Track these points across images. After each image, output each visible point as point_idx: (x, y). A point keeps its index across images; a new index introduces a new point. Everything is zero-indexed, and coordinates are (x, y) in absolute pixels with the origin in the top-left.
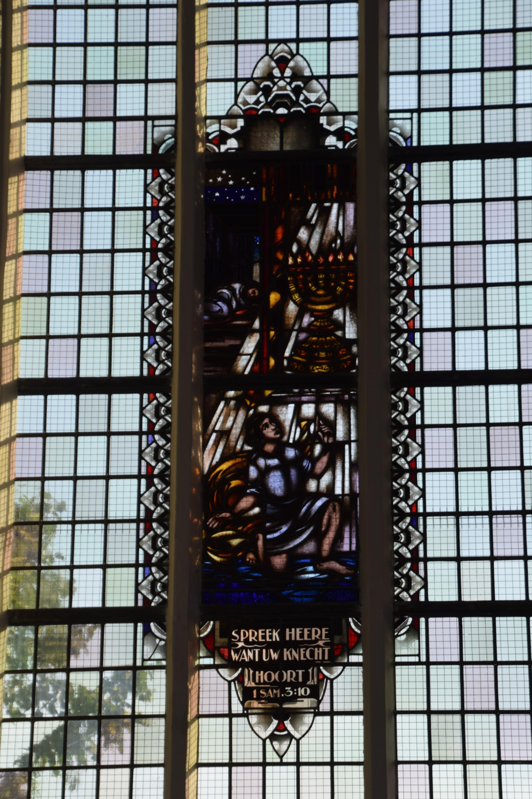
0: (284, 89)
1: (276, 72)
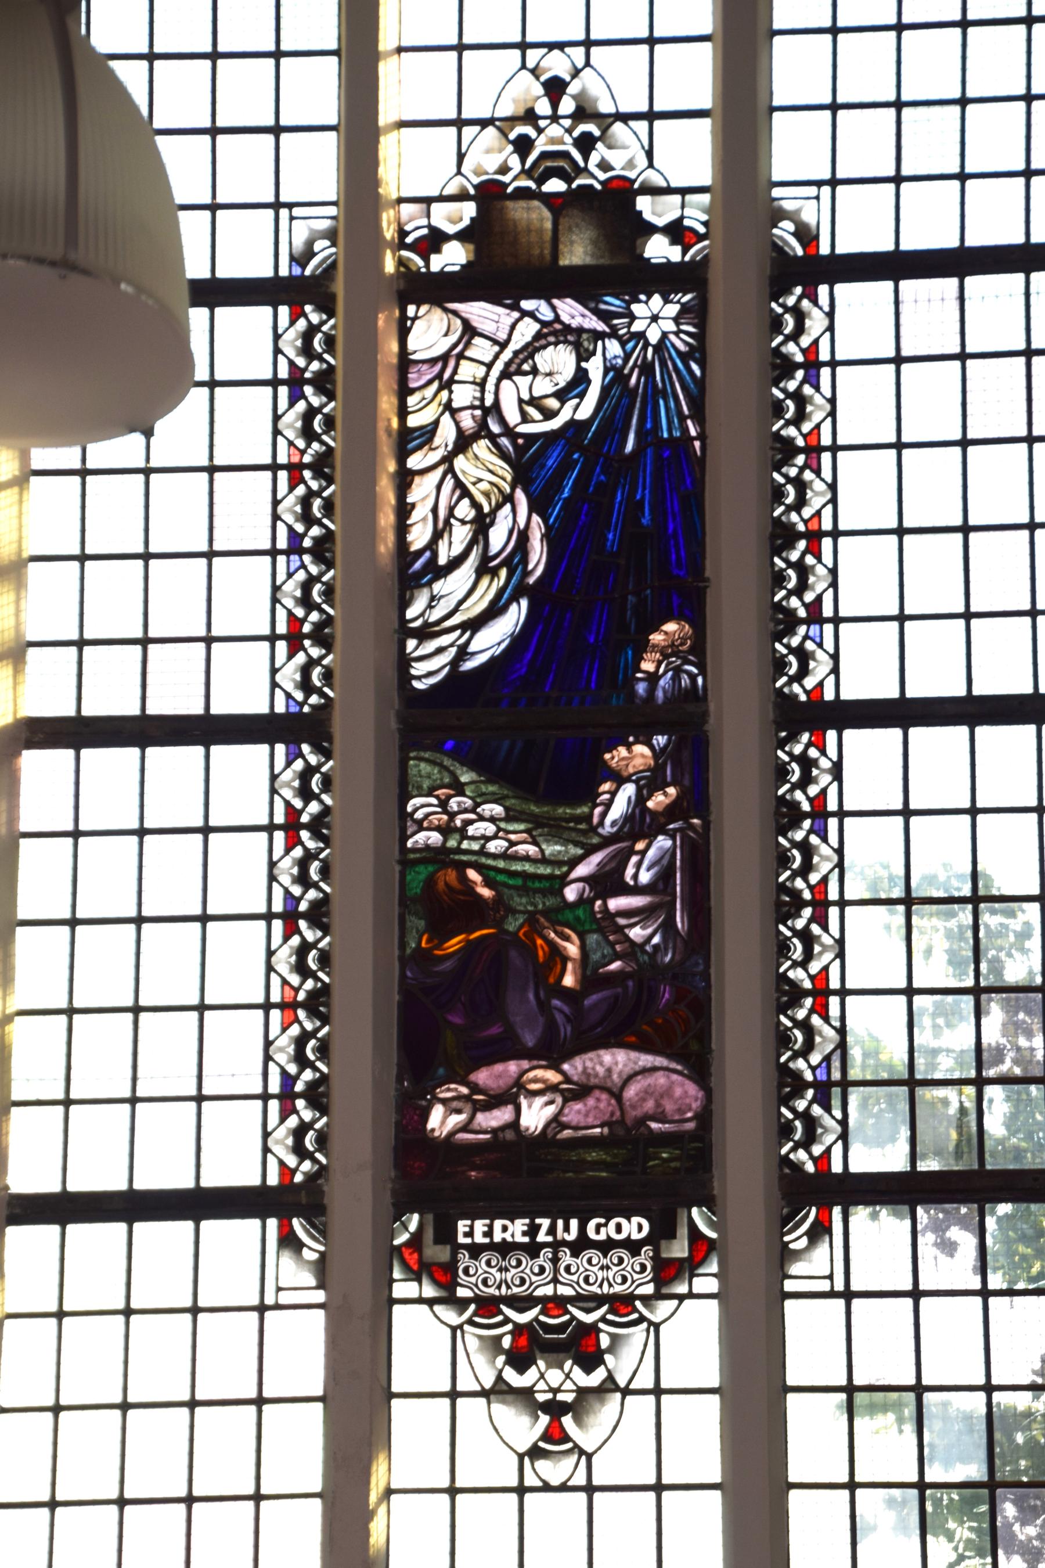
1: (543, 107)
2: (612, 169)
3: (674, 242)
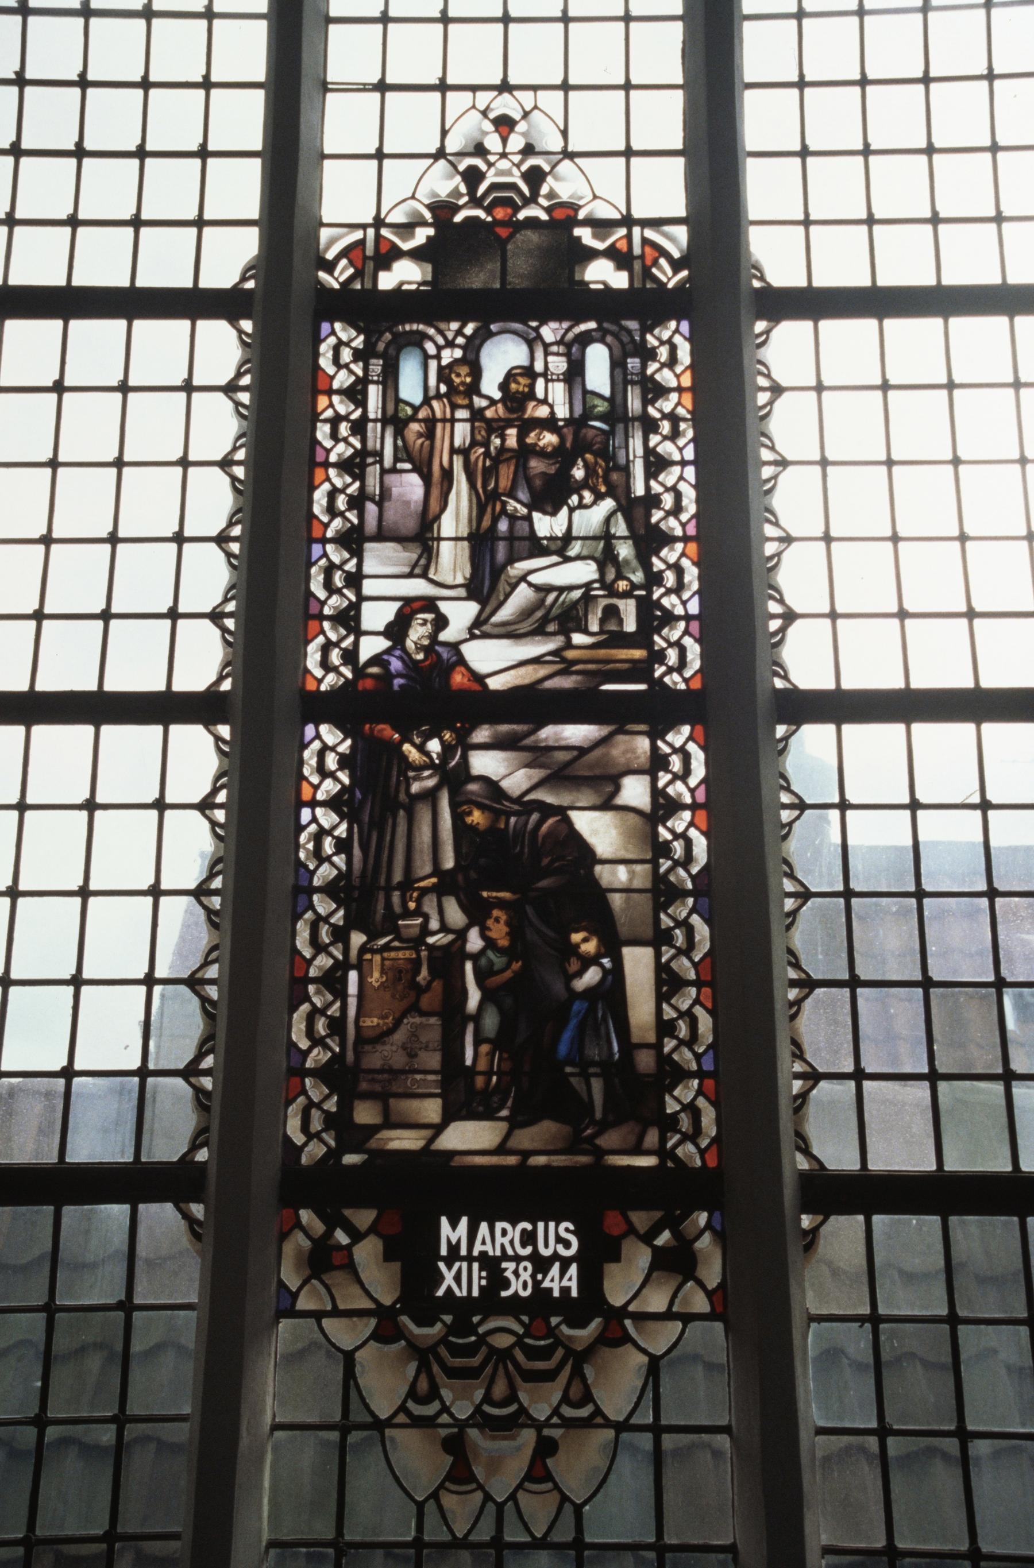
0: (508, 173)
1: (493, 143)
2: (559, 197)
3: (620, 267)
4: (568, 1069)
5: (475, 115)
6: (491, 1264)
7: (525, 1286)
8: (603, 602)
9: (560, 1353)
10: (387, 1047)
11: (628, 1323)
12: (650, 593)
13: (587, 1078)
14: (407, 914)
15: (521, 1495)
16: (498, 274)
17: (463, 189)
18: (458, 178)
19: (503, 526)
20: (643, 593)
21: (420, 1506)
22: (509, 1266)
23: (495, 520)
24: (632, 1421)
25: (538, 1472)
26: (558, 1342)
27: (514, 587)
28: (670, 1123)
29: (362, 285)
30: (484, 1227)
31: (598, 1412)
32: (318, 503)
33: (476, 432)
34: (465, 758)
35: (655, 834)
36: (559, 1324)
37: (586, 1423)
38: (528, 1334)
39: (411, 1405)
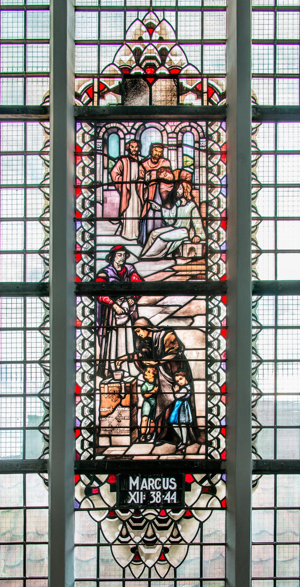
1: (146, 36)
4: (174, 425)
5: (138, 23)
6: (147, 493)
7: (158, 500)
8: (189, 246)
9: (170, 521)
10: (111, 419)
11: (193, 511)
12: (207, 242)
13: (180, 428)
14: (117, 370)
15: (156, 565)
16: (148, 101)
17: (133, 59)
18: (132, 54)
19: (151, 214)
20: (205, 242)
21: (124, 569)
22: (154, 493)
23: (148, 211)
24: (193, 542)
25: (162, 558)
26: (169, 518)
27: (155, 240)
28: (209, 444)
29: (93, 104)
30: (144, 480)
31: (182, 539)
32: (78, 204)
33: (140, 172)
34: (137, 310)
35: (207, 339)
36: (169, 512)
37: (177, 543)
38: (159, 515)
39: (120, 538)
